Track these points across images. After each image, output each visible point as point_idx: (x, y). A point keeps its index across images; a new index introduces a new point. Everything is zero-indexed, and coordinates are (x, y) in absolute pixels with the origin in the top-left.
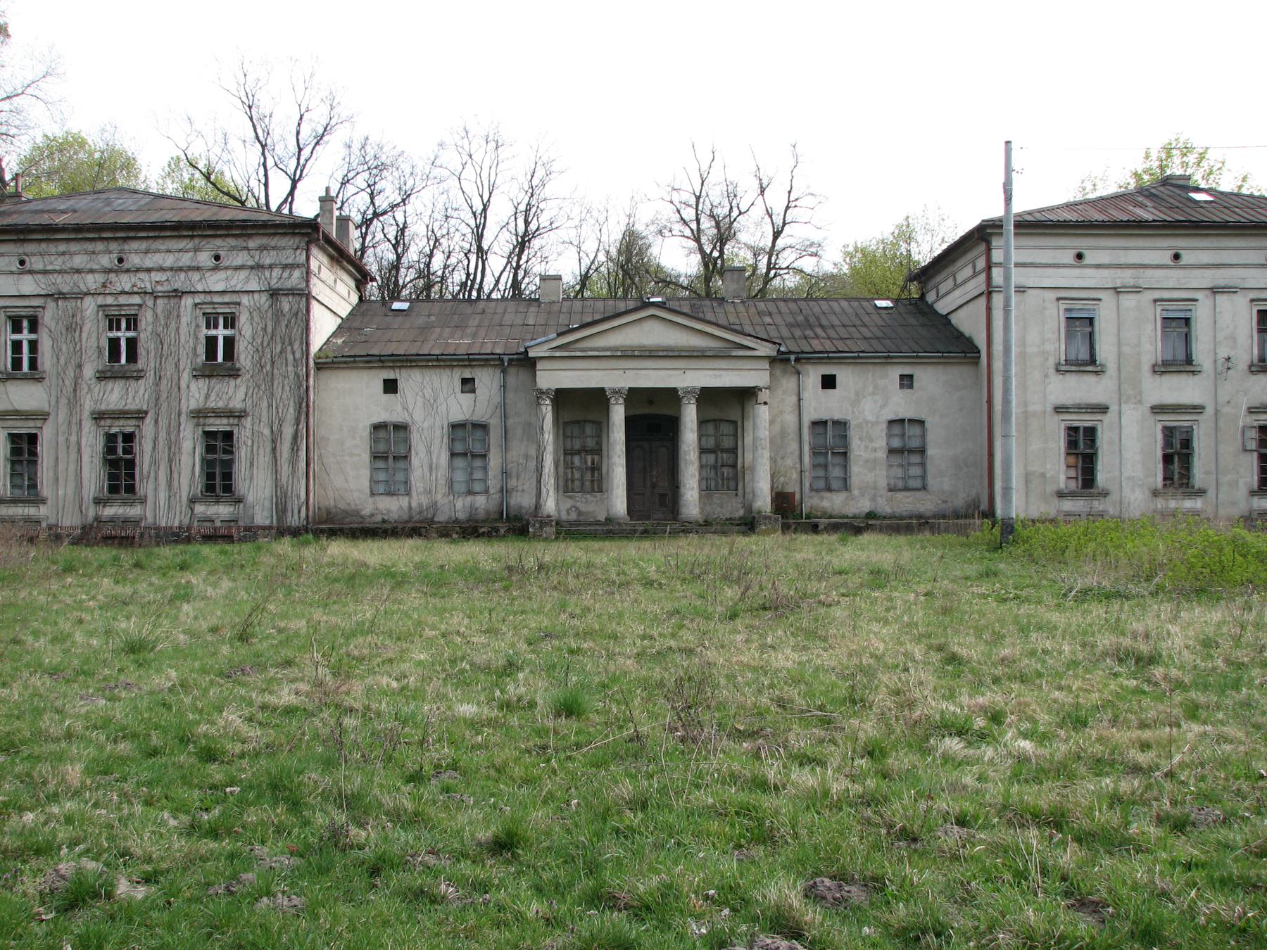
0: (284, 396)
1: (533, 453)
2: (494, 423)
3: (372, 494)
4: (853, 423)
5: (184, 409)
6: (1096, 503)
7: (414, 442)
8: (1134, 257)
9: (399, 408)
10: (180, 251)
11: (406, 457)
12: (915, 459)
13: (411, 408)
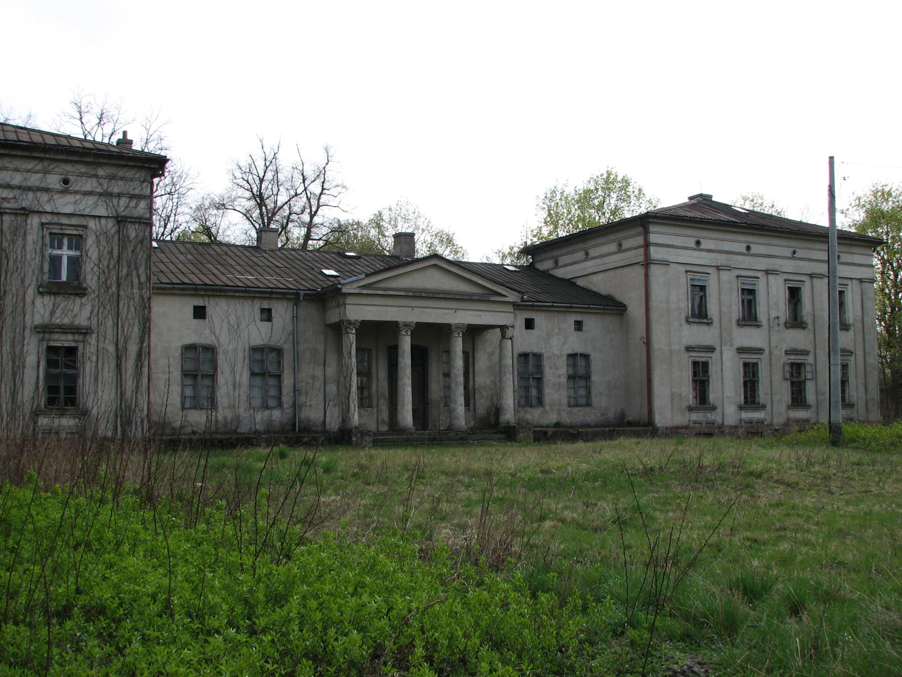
0: (130, 316)
2: (287, 347)
3: (183, 408)
4: (546, 355)
5: (28, 324)
6: (709, 415)
7: (220, 362)
8: (726, 246)
9: (207, 332)
10: (29, 171)
11: (213, 377)
12: (582, 383)
13: (217, 333)
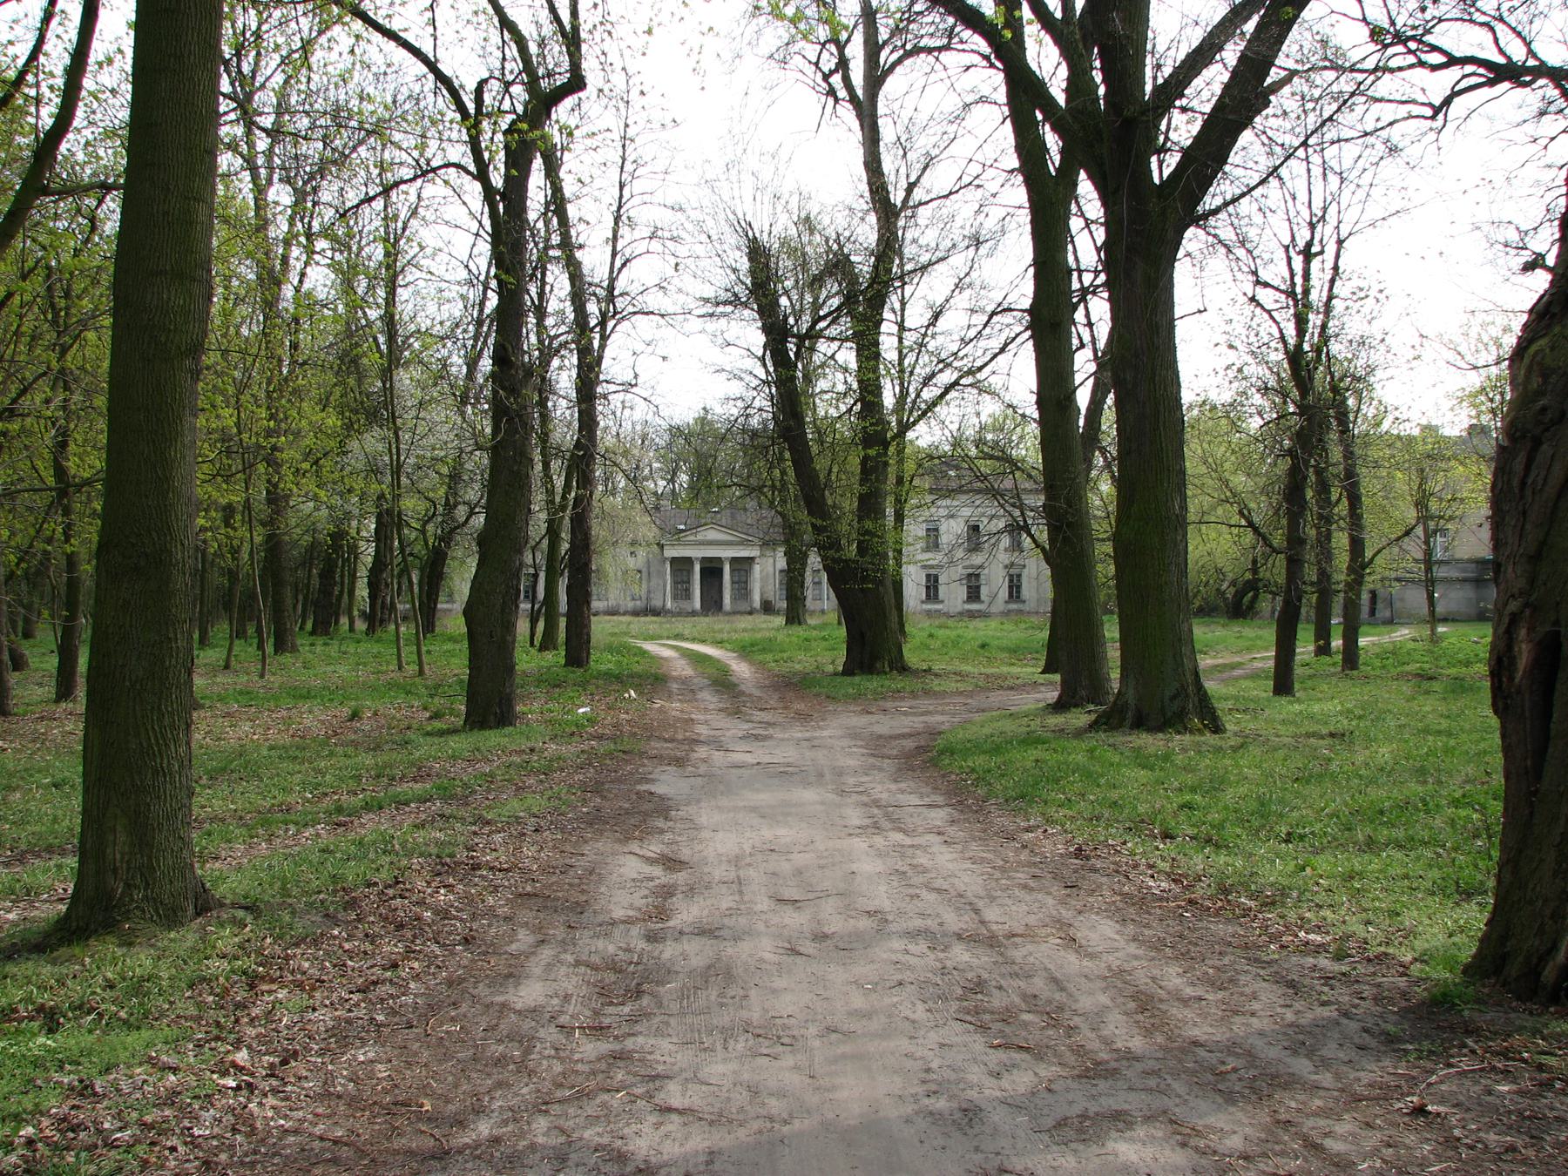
1: (661, 582)
